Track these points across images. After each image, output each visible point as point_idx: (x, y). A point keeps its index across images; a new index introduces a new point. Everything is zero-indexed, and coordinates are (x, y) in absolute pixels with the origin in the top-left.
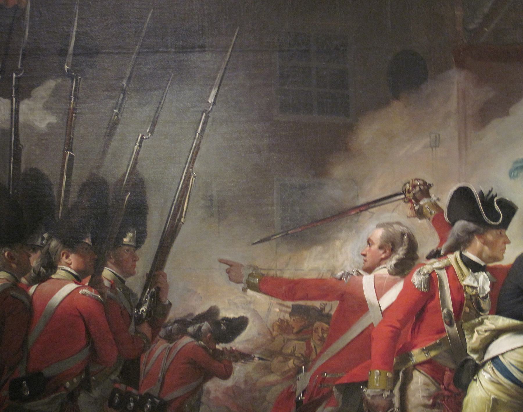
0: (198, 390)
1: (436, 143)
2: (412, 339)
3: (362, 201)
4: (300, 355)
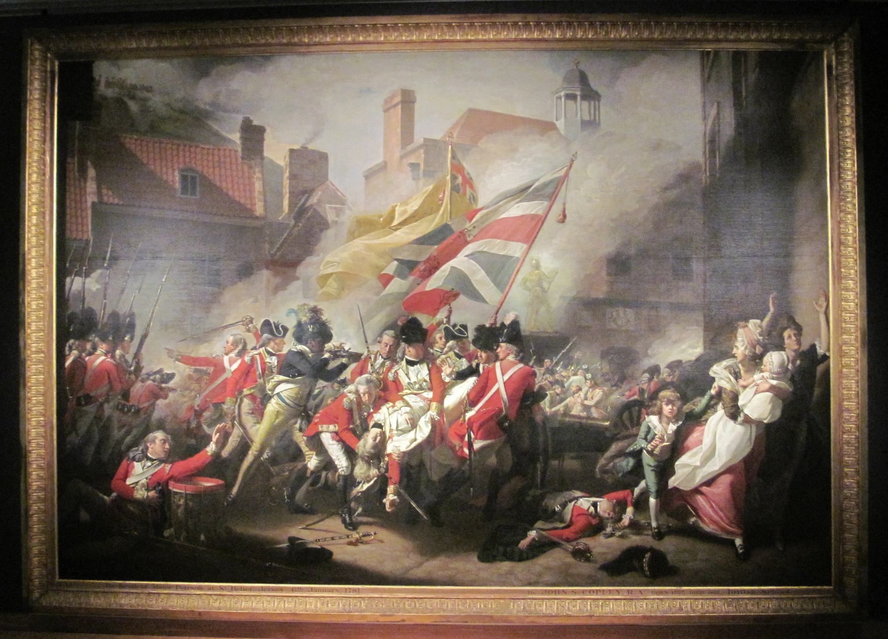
0: (153, 405)
1: (256, 301)
3: (225, 324)
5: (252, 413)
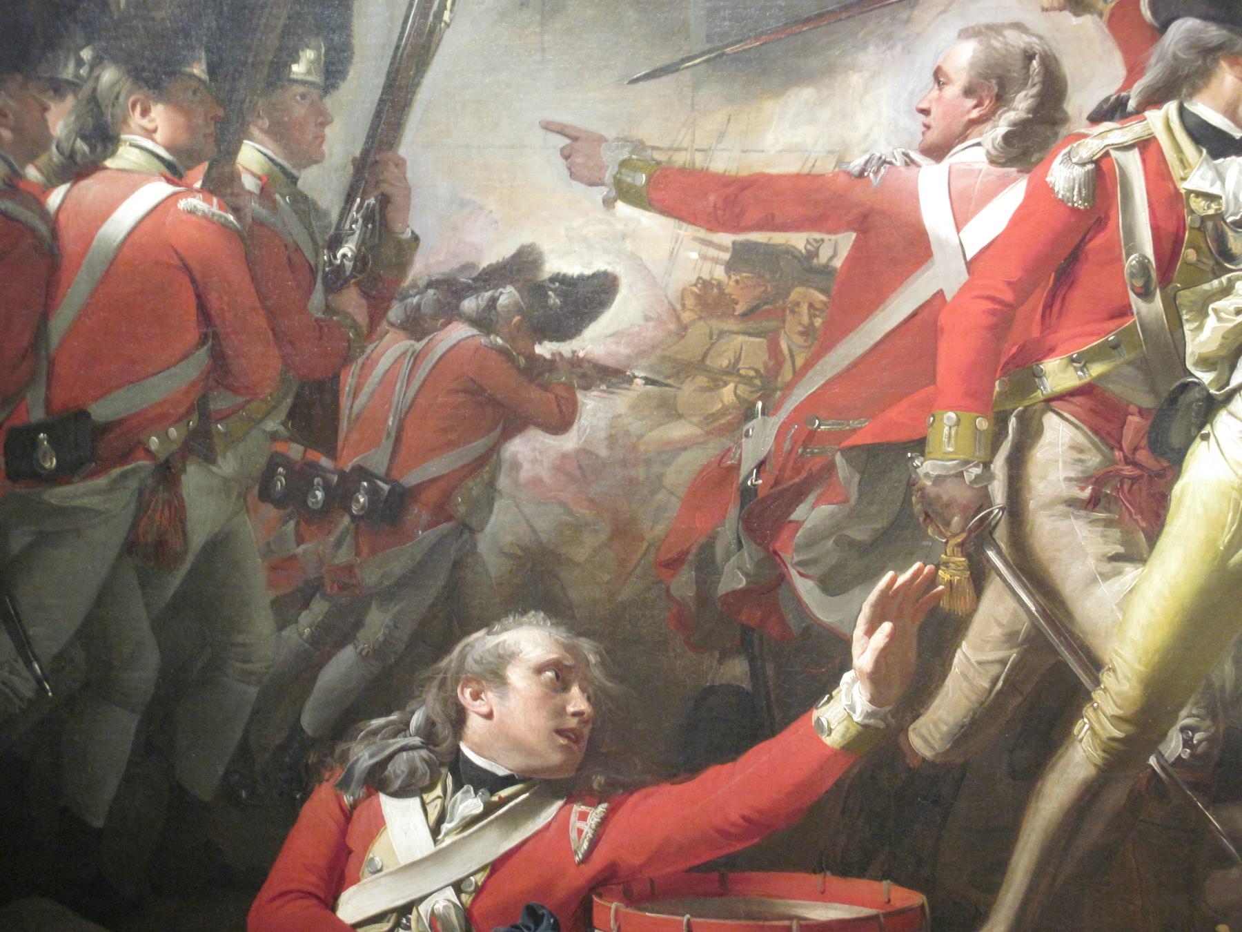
0: (486, 462)
2: (1042, 332)
4: (752, 373)
5: (1093, 503)
